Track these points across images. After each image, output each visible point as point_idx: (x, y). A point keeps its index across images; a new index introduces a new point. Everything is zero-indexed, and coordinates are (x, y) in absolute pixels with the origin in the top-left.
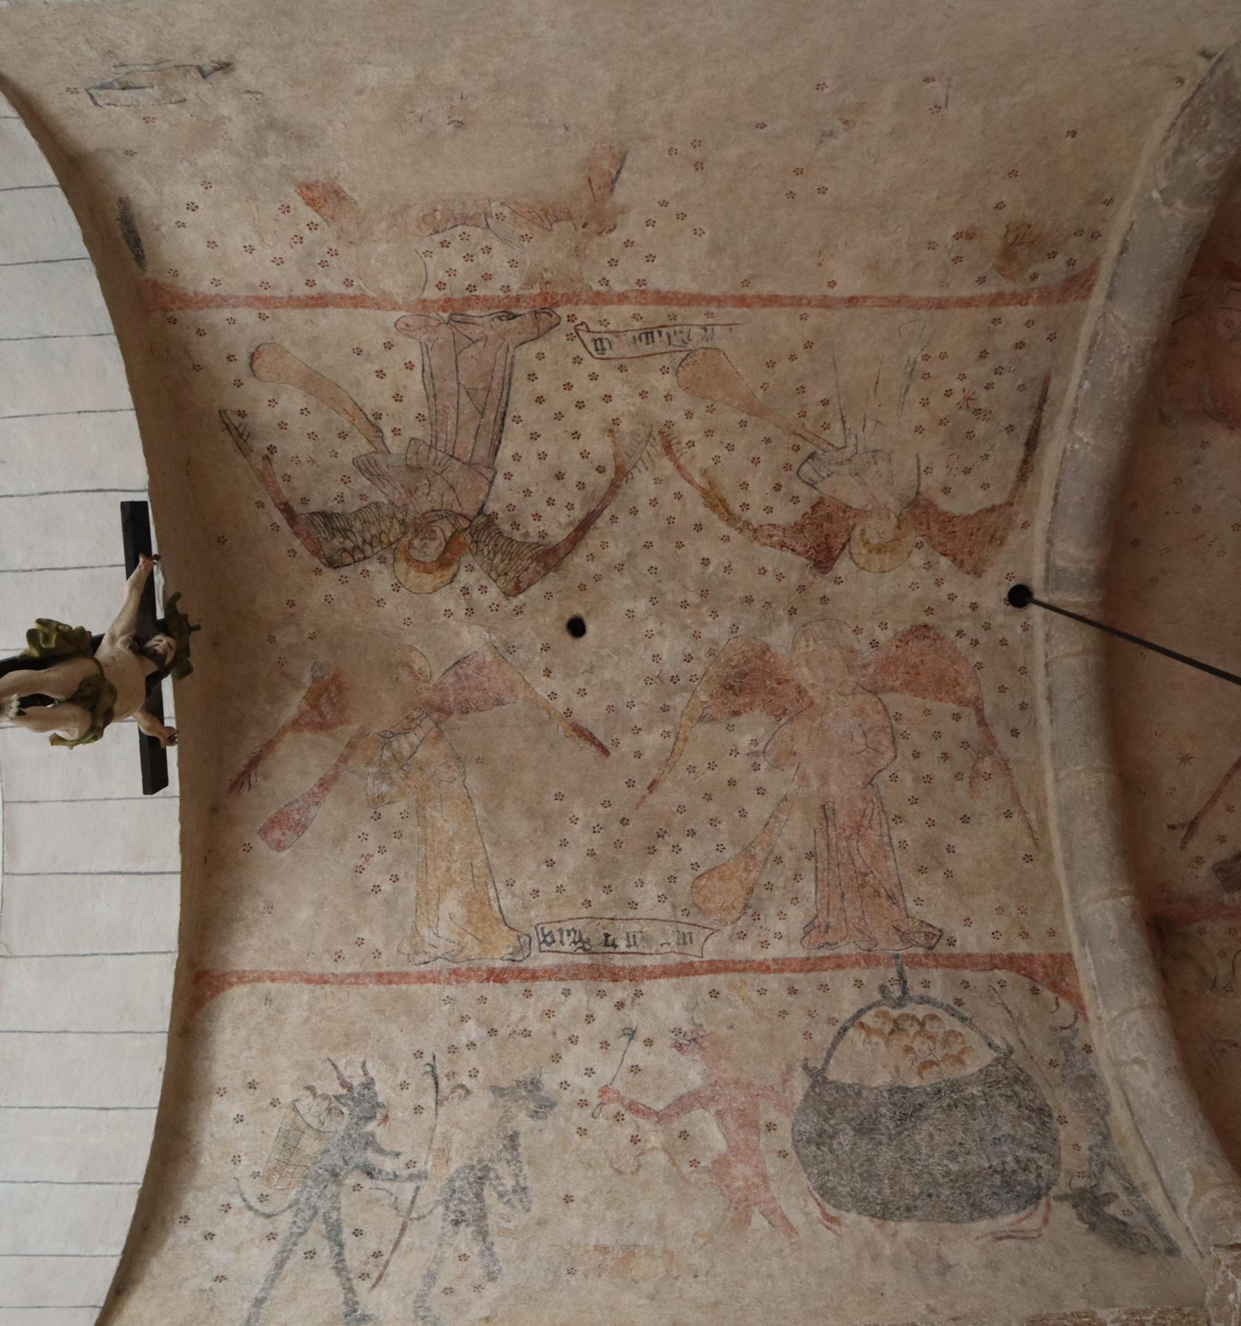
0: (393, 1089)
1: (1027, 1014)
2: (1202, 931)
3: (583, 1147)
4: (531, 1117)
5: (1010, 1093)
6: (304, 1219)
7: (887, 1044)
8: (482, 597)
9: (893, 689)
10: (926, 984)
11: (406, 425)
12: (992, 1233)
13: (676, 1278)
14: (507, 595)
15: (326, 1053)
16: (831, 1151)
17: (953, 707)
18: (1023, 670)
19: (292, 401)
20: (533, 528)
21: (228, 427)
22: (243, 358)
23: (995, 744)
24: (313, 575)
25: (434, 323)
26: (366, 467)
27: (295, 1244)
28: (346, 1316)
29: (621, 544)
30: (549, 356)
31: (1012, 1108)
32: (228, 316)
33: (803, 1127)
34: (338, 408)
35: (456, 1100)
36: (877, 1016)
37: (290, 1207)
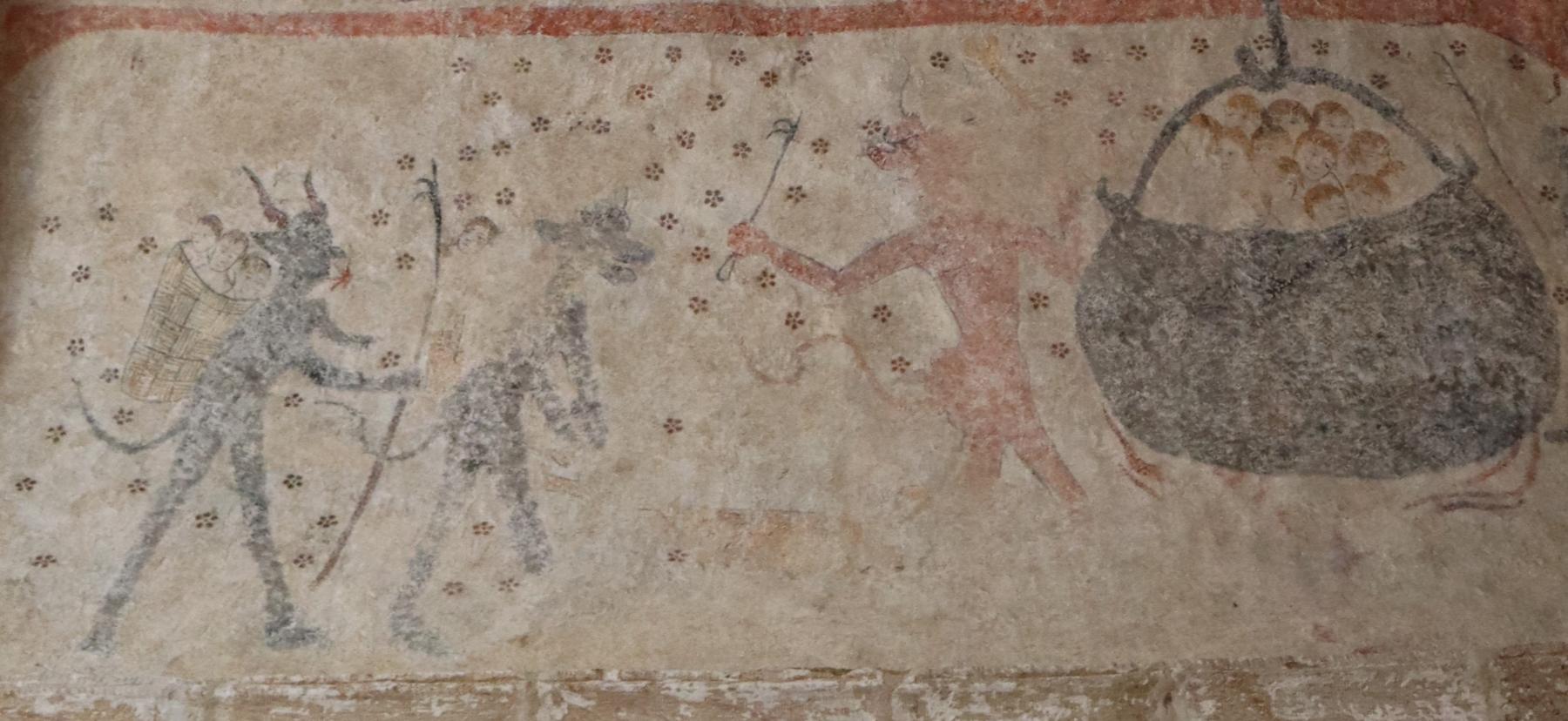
0: (360, 224)
1: (1501, 103)
3: (701, 333)
4: (608, 277)
5: (1469, 246)
6: (196, 456)
7: (1250, 155)
10: (1321, 48)
12: (1434, 498)
13: (863, 572)
15: (240, 158)
16: (1147, 346)
27: (179, 500)
28: (269, 631)
31: (1473, 273)
33: (1098, 302)
35: (473, 246)
36: (1232, 103)
37: (171, 433)
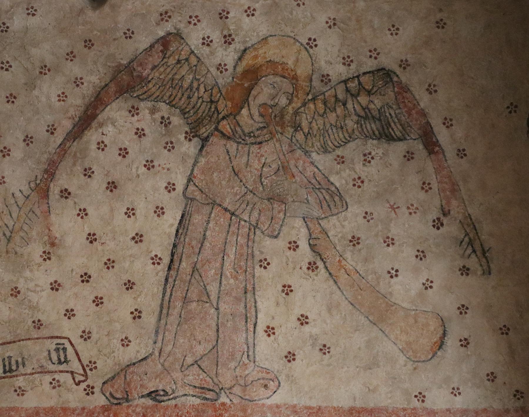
8: (208, 32)
11: (282, 254)
14: (178, 35)
19: (404, 289)
20: (145, 119)
21: (484, 253)
22: (451, 342)
24: (411, 61)
25: (237, 390)
26: (333, 199)
29: (44, 99)
30: (116, 343)
32: (458, 398)
34: (356, 277)
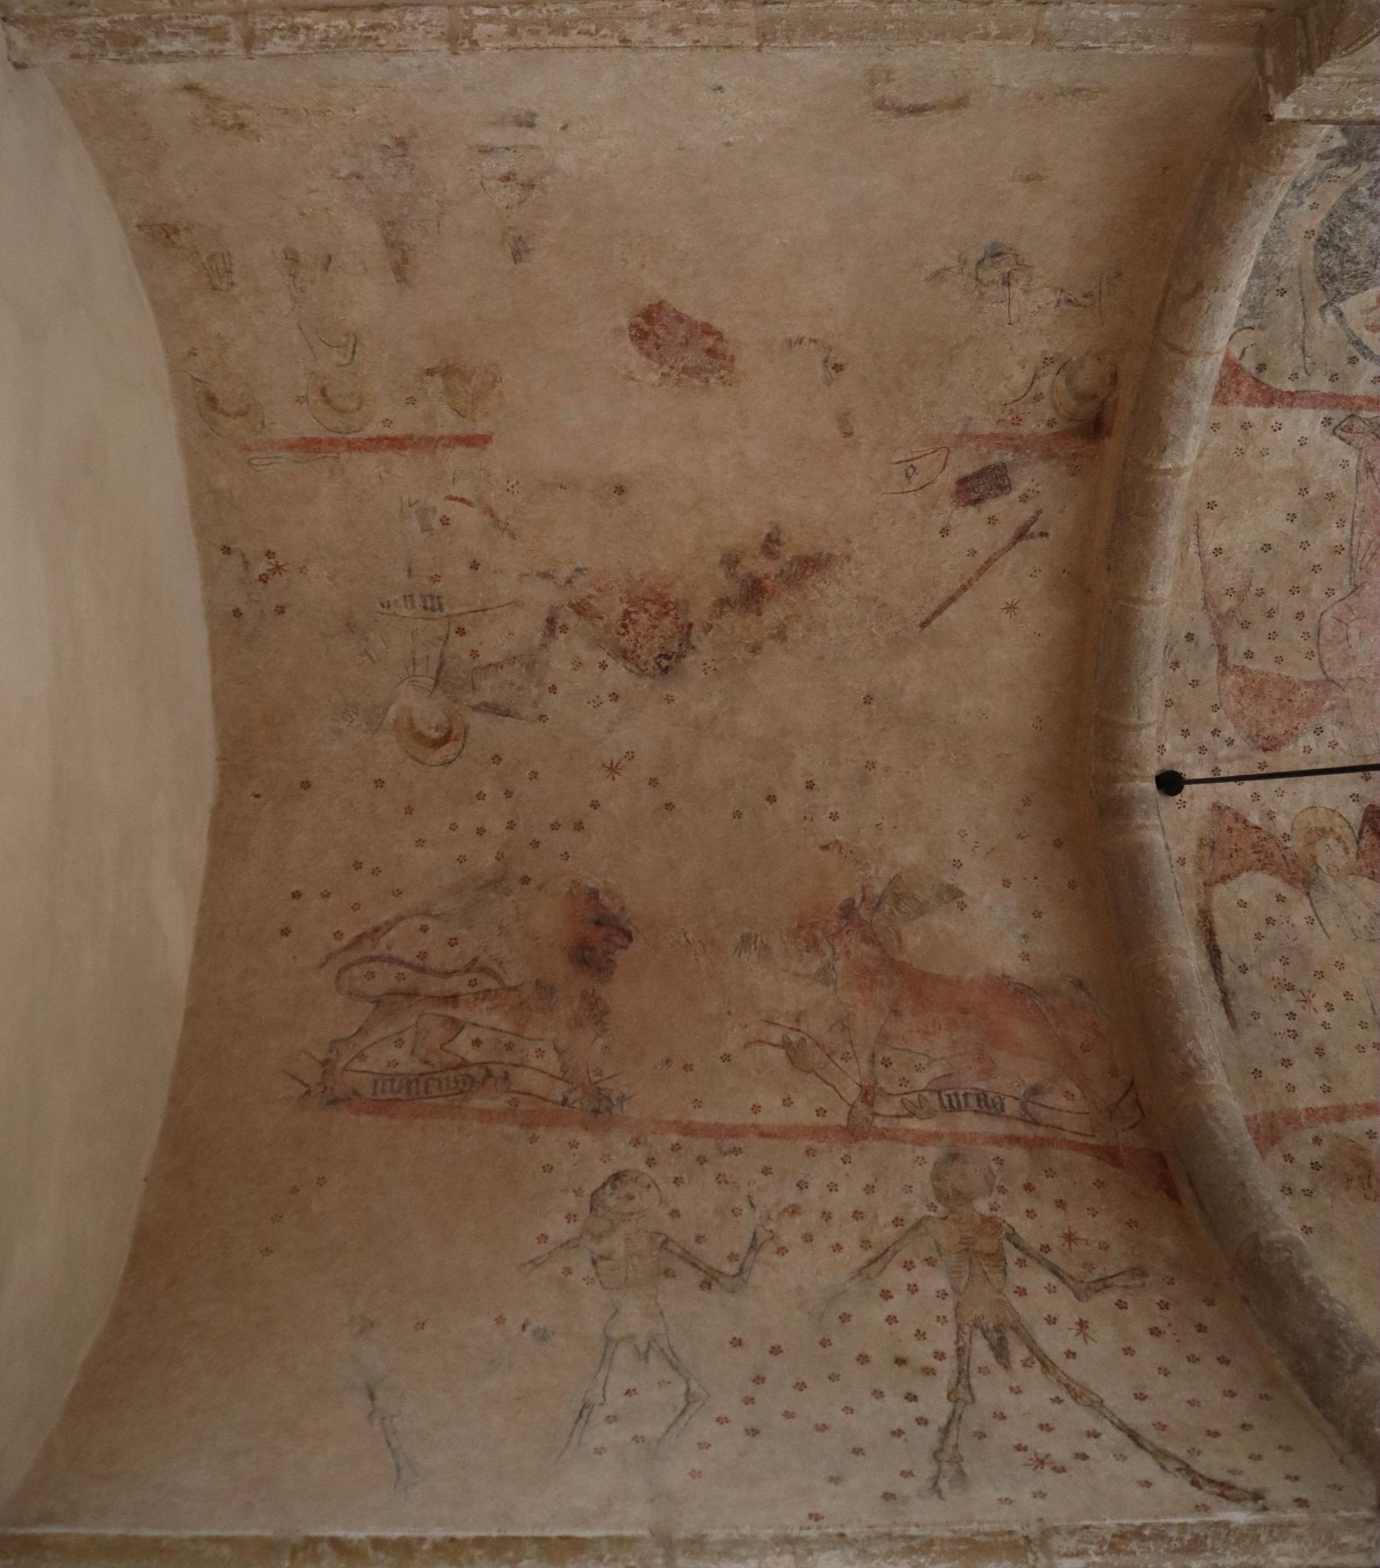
2: (1051, 423)
9: (1308, 684)
17: (1252, 666)
18: (1169, 703)
23: (1213, 625)
